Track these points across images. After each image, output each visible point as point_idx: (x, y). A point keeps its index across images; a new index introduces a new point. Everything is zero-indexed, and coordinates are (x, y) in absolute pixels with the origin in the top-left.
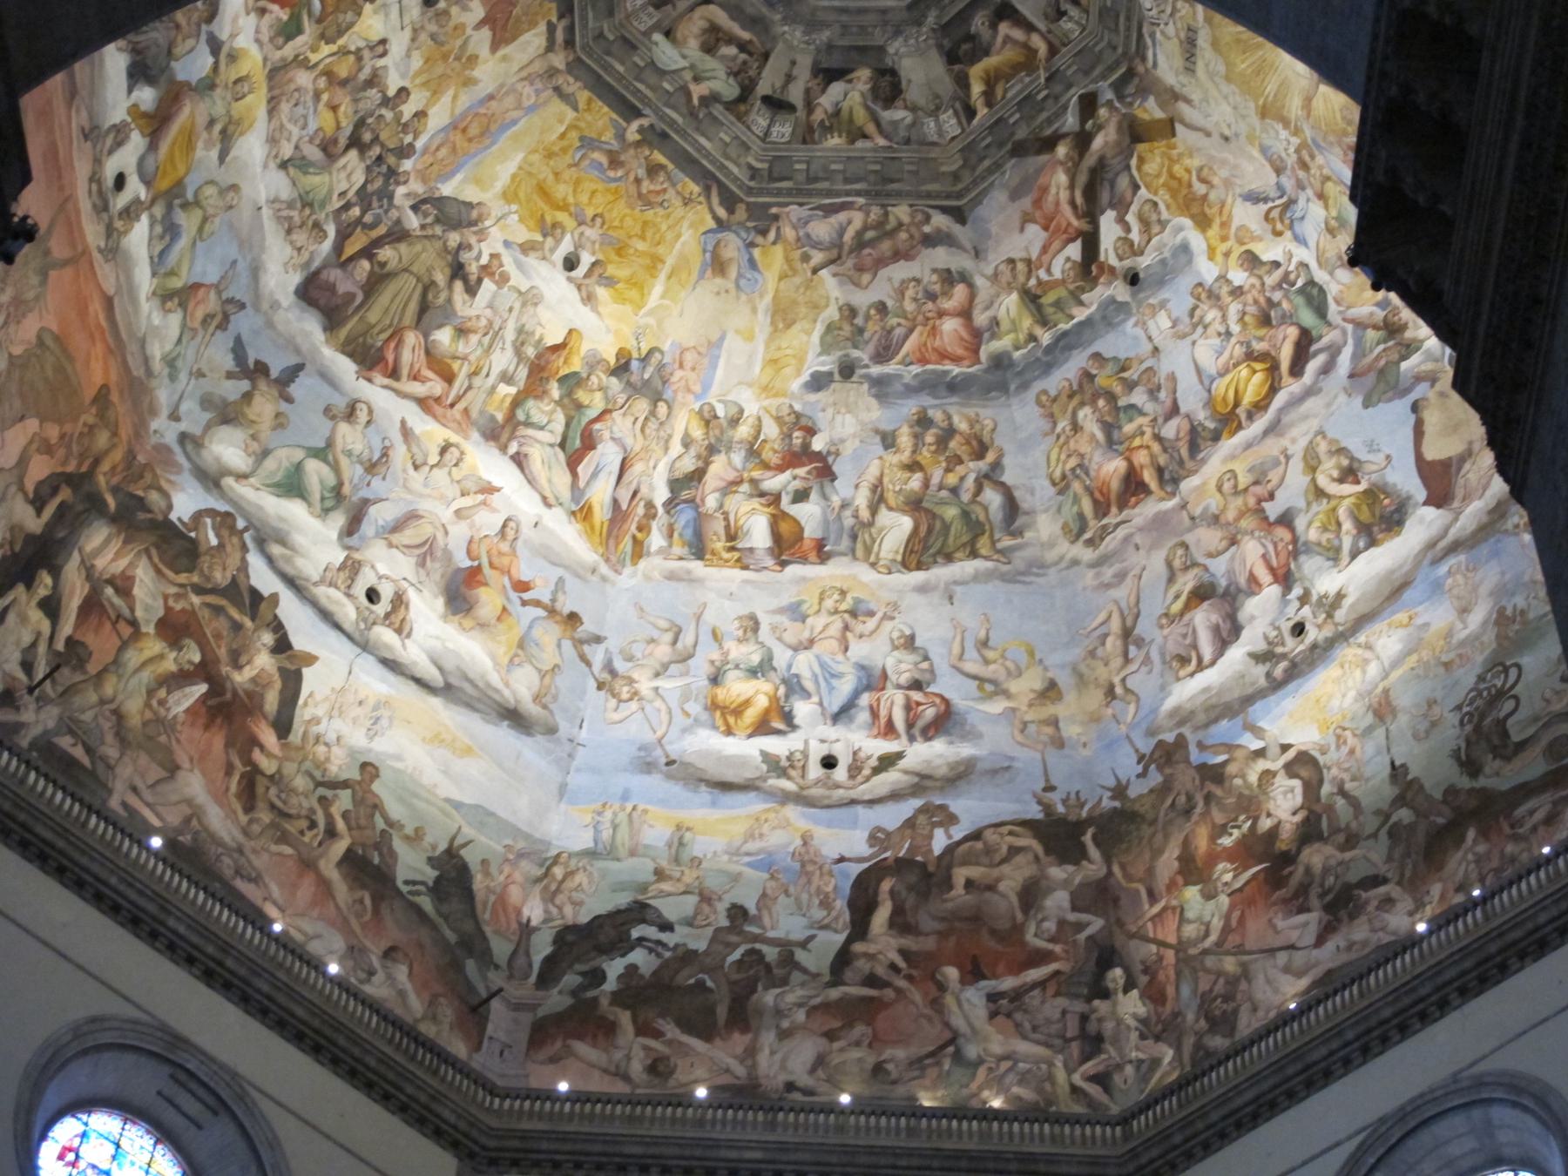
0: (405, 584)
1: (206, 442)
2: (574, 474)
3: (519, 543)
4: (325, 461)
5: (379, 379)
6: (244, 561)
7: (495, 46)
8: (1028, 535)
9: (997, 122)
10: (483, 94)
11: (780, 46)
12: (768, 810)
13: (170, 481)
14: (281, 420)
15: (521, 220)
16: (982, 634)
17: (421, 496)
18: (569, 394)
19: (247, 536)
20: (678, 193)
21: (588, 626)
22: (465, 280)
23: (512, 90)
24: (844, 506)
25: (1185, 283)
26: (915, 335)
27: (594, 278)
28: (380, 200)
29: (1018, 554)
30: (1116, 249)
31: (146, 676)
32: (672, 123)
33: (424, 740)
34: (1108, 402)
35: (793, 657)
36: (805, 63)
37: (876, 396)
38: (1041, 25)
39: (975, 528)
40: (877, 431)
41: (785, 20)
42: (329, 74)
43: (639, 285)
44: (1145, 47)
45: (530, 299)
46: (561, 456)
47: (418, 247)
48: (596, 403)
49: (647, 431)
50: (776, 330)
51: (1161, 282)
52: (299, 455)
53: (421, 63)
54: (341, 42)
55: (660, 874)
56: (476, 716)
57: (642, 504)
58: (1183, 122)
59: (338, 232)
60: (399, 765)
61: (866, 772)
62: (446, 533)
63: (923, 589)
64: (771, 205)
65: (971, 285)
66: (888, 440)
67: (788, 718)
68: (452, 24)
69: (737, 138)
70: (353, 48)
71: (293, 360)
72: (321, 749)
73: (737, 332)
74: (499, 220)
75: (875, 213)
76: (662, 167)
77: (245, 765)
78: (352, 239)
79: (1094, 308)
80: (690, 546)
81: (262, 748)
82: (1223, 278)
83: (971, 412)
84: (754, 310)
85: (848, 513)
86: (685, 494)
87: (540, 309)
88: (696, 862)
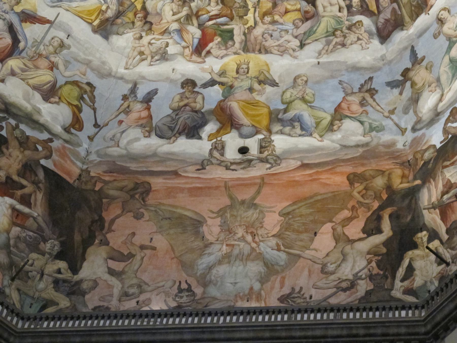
52: (447, 59)
54: (250, 6)
59: (361, 14)
78: (369, 5)
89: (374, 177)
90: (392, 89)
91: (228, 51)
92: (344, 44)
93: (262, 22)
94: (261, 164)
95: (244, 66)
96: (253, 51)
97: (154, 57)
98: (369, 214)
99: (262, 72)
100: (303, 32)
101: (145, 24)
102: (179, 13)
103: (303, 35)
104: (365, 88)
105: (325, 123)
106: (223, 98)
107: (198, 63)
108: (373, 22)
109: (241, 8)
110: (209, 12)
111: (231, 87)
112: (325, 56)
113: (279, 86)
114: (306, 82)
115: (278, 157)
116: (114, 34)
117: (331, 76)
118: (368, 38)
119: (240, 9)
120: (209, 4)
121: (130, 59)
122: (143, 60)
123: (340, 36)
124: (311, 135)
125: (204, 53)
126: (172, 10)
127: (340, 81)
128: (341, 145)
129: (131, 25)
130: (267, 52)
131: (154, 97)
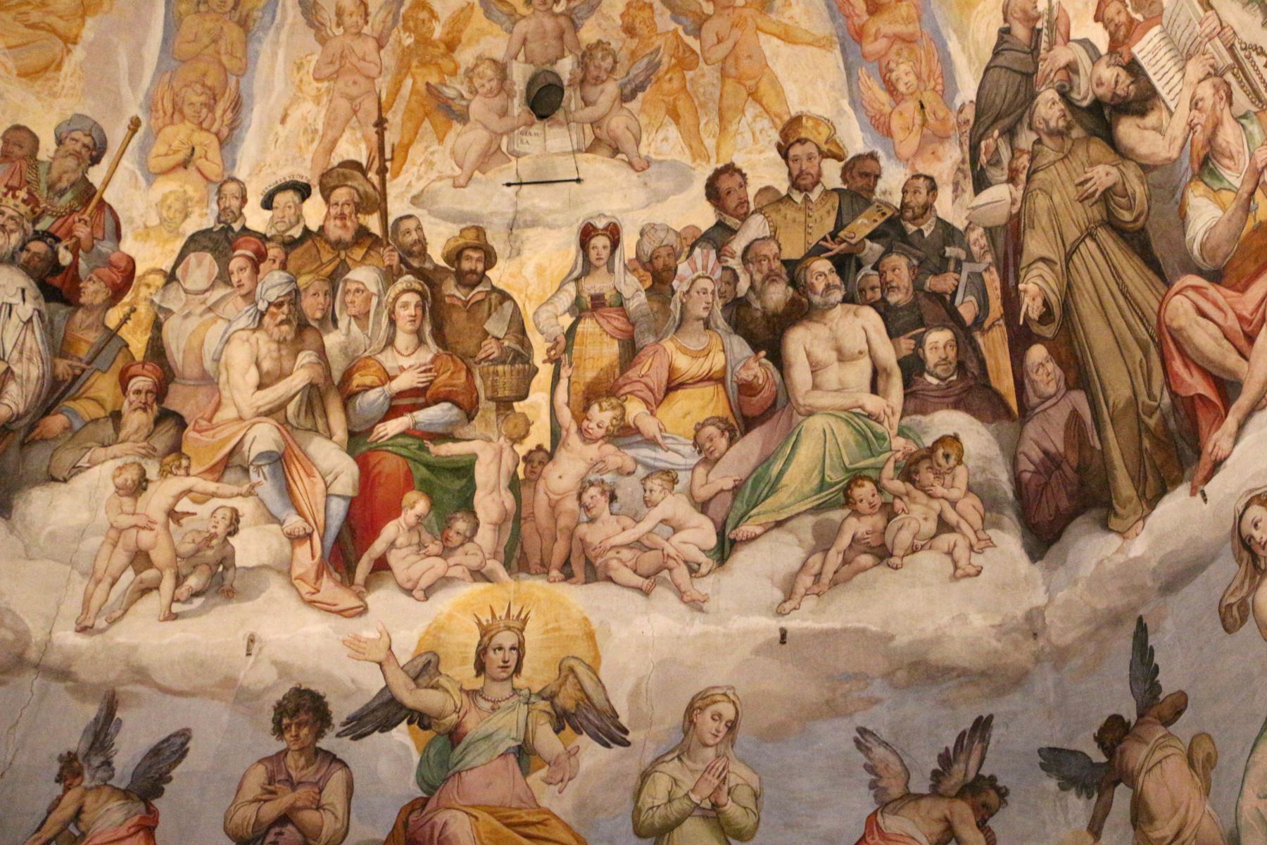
5: (1218, 441)
14: (1200, 756)
28: (940, 270)
42: (593, 394)
47: (1041, 202)
53: (672, 131)
54: (539, 357)
59: (956, 406)
68: (617, 41)
70: (567, 321)
78: (990, 363)
90: (1063, 788)
91: (452, 561)
92: (883, 545)
93: (580, 430)
95: (507, 639)
96: (543, 564)
97: (186, 577)
99: (572, 670)
100: (728, 484)
101: (158, 421)
102: (282, 375)
103: (729, 496)
106: (420, 794)
107: (340, 612)
108: (1002, 449)
109: (504, 363)
110: (391, 378)
111: (454, 736)
112: (810, 603)
113: (627, 744)
114: (732, 726)
116: (36, 483)
117: (827, 702)
118: (977, 522)
119: (500, 368)
120: (390, 342)
121: (99, 582)
122: (146, 590)
123: (872, 506)
126: (258, 365)
127: (862, 731)
129: (109, 429)
130: (594, 573)
131: (174, 773)
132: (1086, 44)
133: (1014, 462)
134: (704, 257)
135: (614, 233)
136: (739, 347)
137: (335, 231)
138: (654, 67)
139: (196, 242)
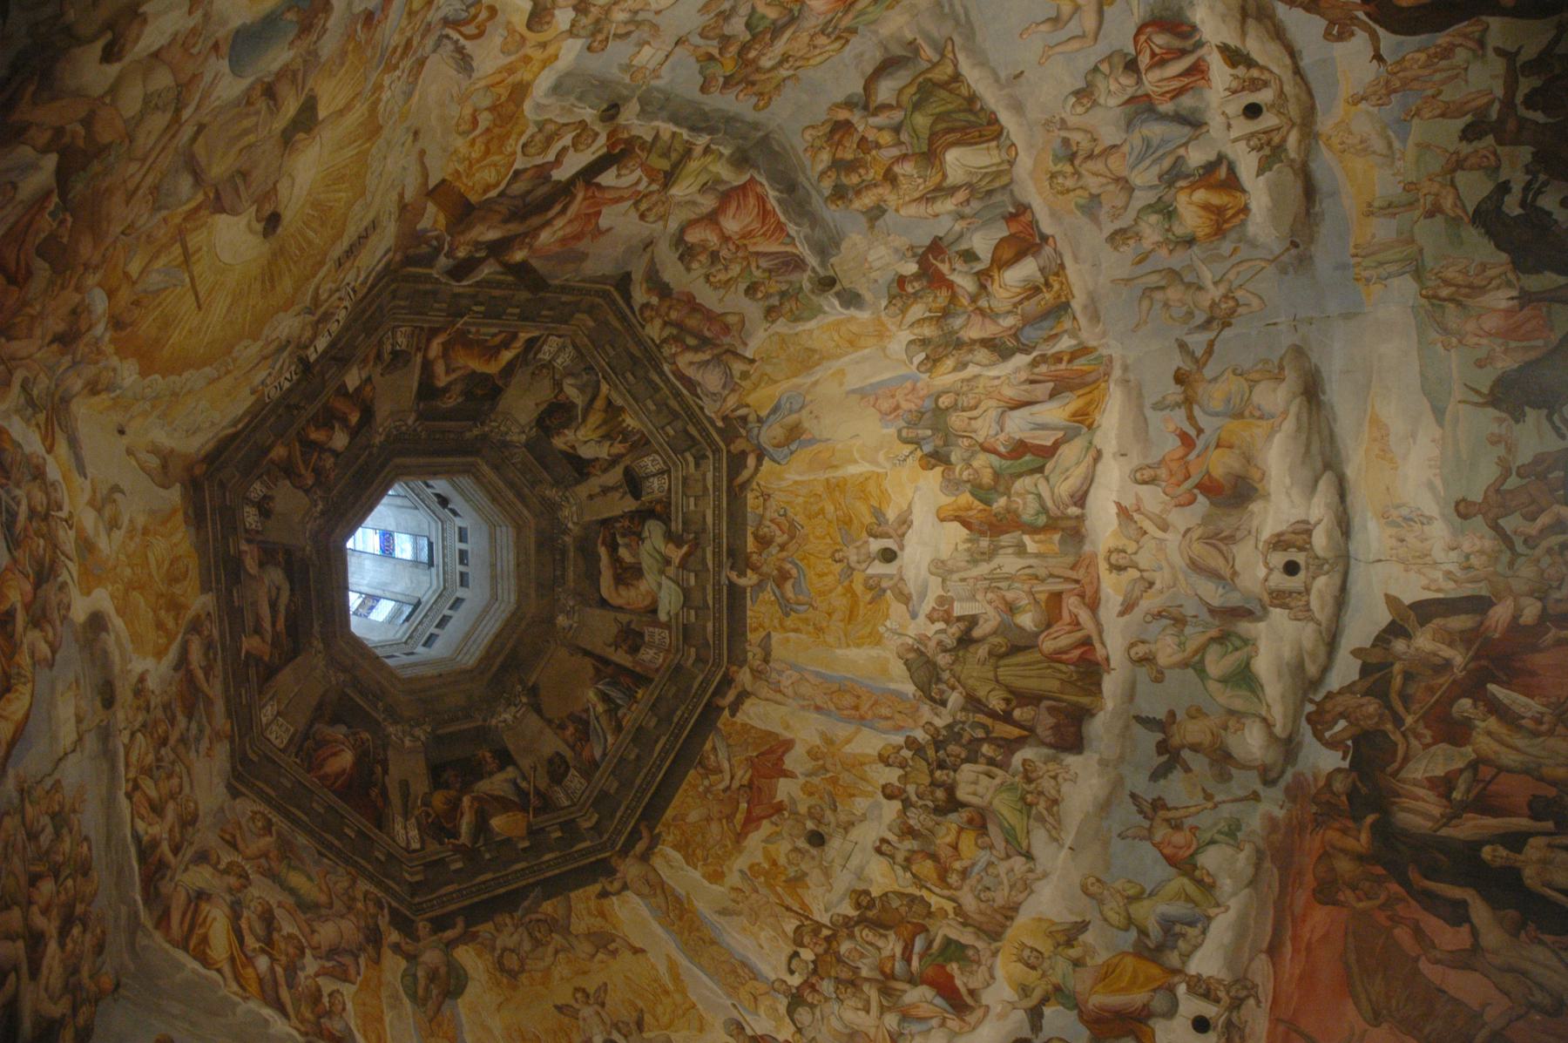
0: (1260, 545)
1: (1259, 763)
2: (1056, 445)
3: (1149, 461)
4: (1202, 661)
5: (1100, 652)
6: (1341, 692)
7: (788, 745)
8: (909, 36)
9: (526, 319)
10: (822, 718)
11: (587, 518)
12: (1329, 147)
13: (1316, 779)
15: (887, 617)
16: (1043, 28)
17: (1172, 567)
18: (993, 489)
19: (1318, 697)
20: (765, 509)
21: (1178, 361)
22: (969, 630)
23: (797, 695)
24: (962, 217)
25: (595, 64)
26: (760, 249)
27: (884, 529)
28: (960, 735)
29: (936, 35)
30: (589, 146)
31: (1519, 741)
32: (717, 554)
33: (1396, 469)
34: (750, 48)
35: (1141, 188)
36: (583, 490)
37: (837, 245)
38: (419, 359)
39: (926, 91)
40: (872, 227)
41: (566, 531)
43: (862, 487)
44: (378, 274)
45: (941, 569)
46: (1049, 466)
47: (970, 682)
48: (981, 460)
49: (973, 402)
50: (822, 359)
51: (604, 84)
52: (1213, 686)
53: (858, 800)
54: (917, 893)
55: (1430, 214)
56: (1337, 430)
57: (1036, 370)
58: (426, 183)
59: (1013, 753)
60: (1438, 483)
61: (1255, 73)
62: (1188, 530)
63: (1018, 107)
64: (715, 427)
65: (682, 230)
66: (876, 214)
67: (1210, 167)
68: (814, 801)
69: (684, 493)
70: (908, 875)
71: (1138, 729)
72: (1474, 560)
73: (841, 384)
74: (901, 635)
75: (668, 350)
76: (756, 536)
77: (1548, 631)
79: (657, 123)
80: (1059, 318)
81: (1515, 618)
82: (572, 33)
83: (806, 158)
84: (815, 384)
85: (967, 210)
86: (1011, 343)
87: (944, 557)
88: (1409, 187)
89: (1333, 869)
94: (1243, 1010)
95: (1027, 953)
98: (1413, 903)
100: (1003, 844)
102: (868, 1001)
104: (1147, 808)
105: (1191, 888)
111: (1058, 989)
114: (1098, 880)
115: (1236, 982)
120: (879, 949)
124: (1209, 919)
125: (969, 1001)
128: (1247, 886)
132: (937, 632)
133: (1043, 744)
134: (912, 813)
135: (883, 840)
136: (953, 816)
137: (820, 950)
138: (830, 794)
139: (790, 1011)
